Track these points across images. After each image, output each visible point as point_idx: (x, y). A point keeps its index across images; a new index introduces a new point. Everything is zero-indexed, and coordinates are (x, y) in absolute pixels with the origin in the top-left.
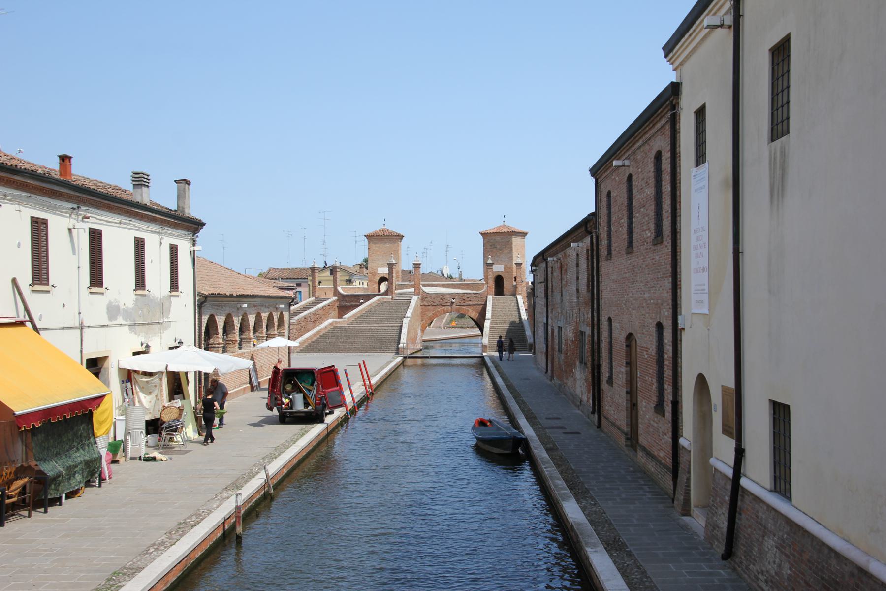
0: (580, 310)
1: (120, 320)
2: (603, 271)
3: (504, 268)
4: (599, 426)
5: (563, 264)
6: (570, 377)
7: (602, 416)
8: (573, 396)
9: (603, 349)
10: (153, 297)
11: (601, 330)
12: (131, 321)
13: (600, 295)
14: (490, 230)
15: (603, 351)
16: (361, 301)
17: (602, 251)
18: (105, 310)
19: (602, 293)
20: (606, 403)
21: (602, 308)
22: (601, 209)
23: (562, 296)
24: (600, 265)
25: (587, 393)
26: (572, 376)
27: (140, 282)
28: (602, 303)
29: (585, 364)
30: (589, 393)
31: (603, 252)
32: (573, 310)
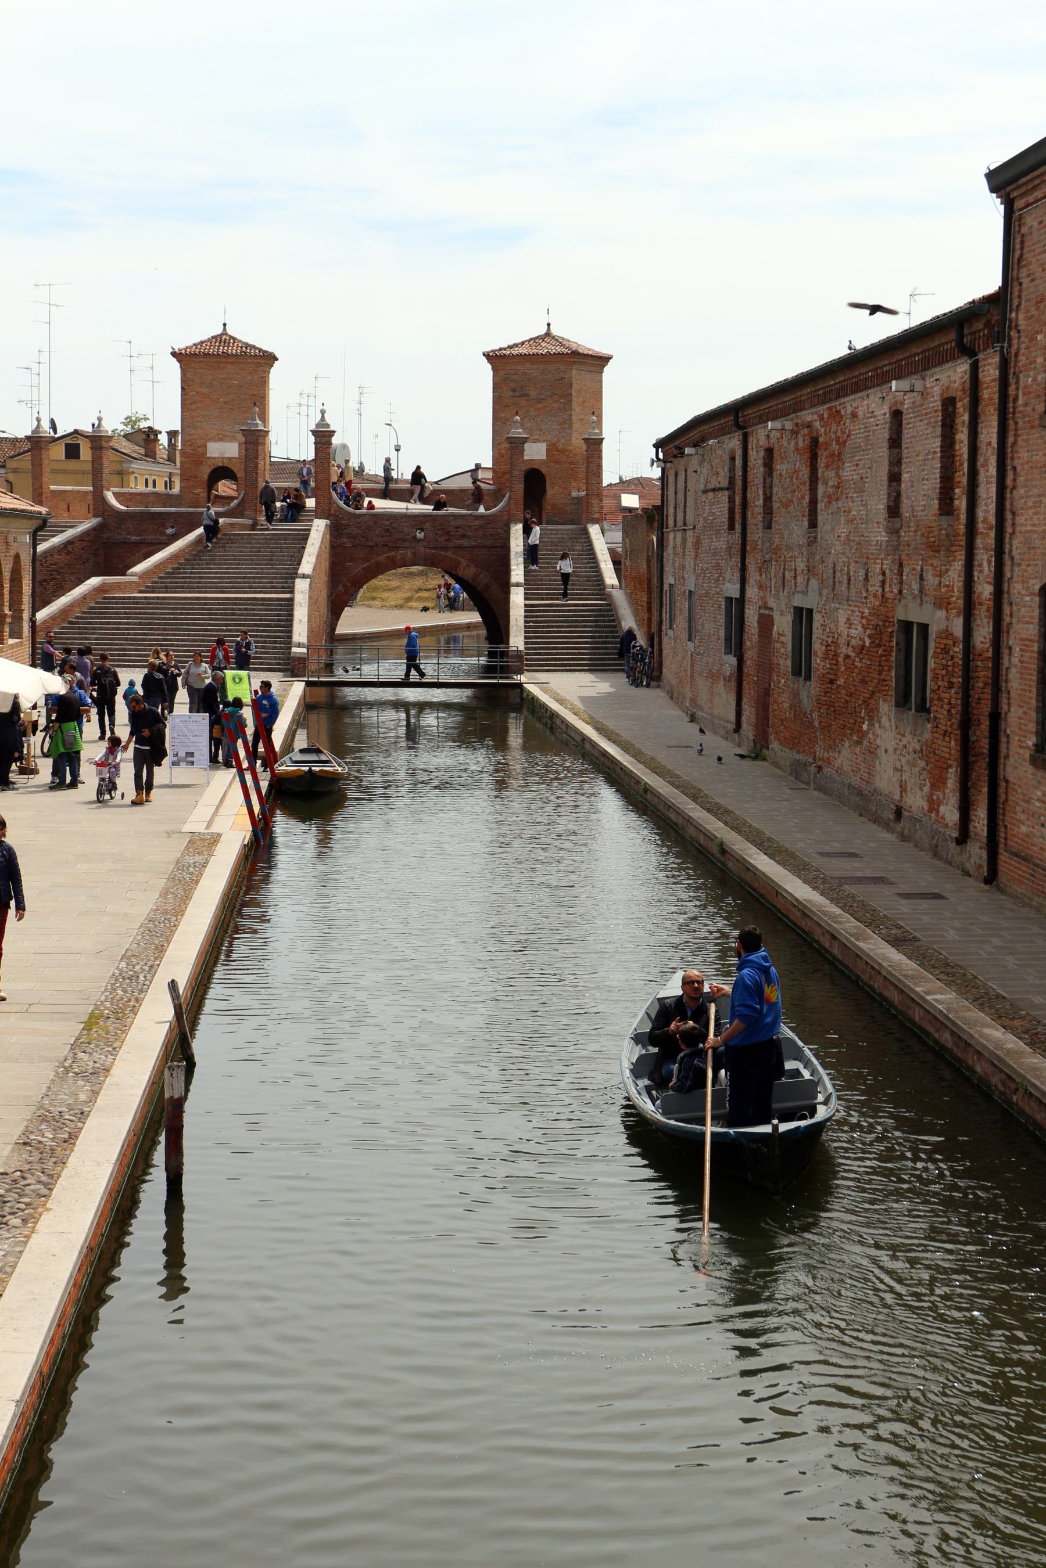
0: (901, 565)
2: (1022, 457)
3: (548, 451)
4: (991, 877)
5: (821, 440)
6: (847, 744)
7: (1001, 851)
8: (860, 793)
9: (1013, 670)
11: (1007, 619)
13: (1008, 524)
14: (516, 345)
15: (1013, 674)
16: (169, 531)
17: (1021, 401)
19: (1013, 519)
20: (1022, 817)
21: (1012, 558)
22: (1021, 284)
23: (813, 524)
24: (1011, 439)
25: (927, 789)
28: (1016, 546)
29: (923, 708)
30: (938, 783)
31: (1026, 405)
32: (866, 564)
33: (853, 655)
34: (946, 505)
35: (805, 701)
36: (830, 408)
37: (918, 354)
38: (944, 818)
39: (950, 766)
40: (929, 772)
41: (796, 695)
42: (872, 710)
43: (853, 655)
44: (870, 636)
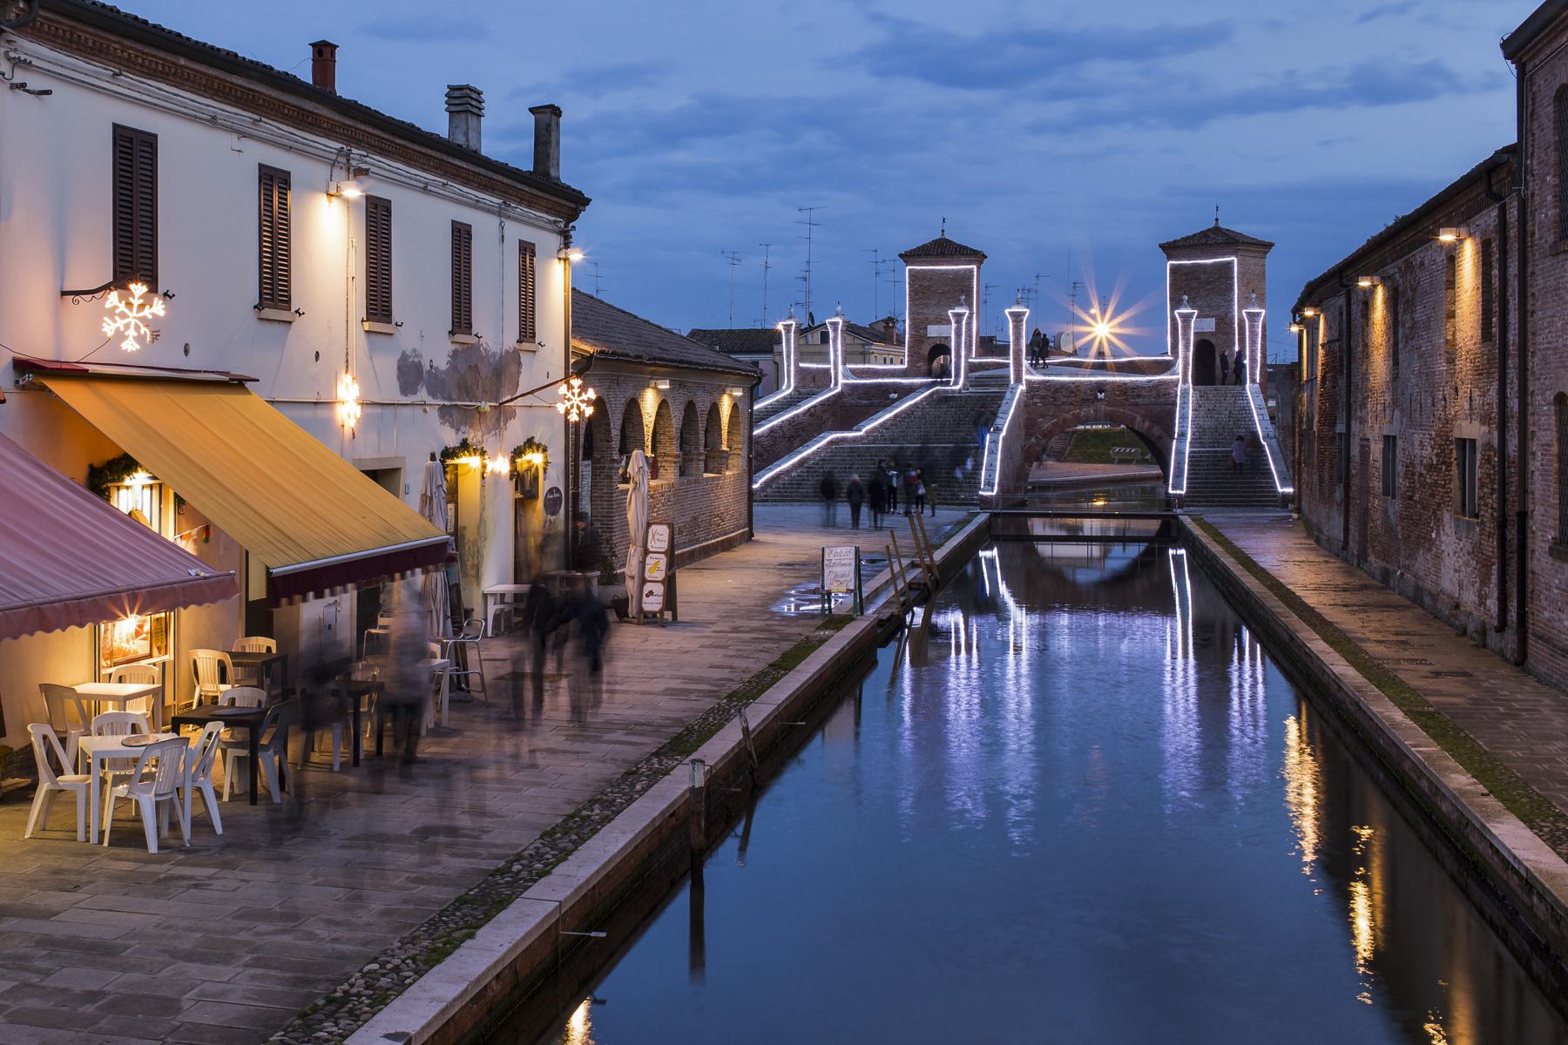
1: (423, 395)
6: (1421, 553)
10: (485, 350)
12: (444, 398)
17: (1537, 236)
18: (394, 372)
22: (1533, 135)
26: (1430, 550)
27: (461, 320)
31: (1540, 238)
33: (1425, 472)
34: (1486, 334)
35: (1392, 517)
36: (1405, 261)
37: (1463, 205)
38: (1489, 610)
39: (1493, 564)
40: (1479, 570)
41: (1385, 511)
42: (1439, 519)
43: (1425, 472)
44: (1437, 455)
